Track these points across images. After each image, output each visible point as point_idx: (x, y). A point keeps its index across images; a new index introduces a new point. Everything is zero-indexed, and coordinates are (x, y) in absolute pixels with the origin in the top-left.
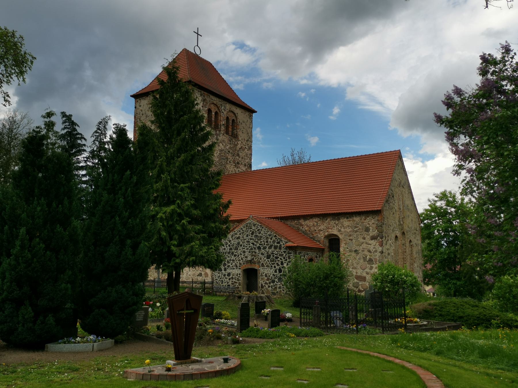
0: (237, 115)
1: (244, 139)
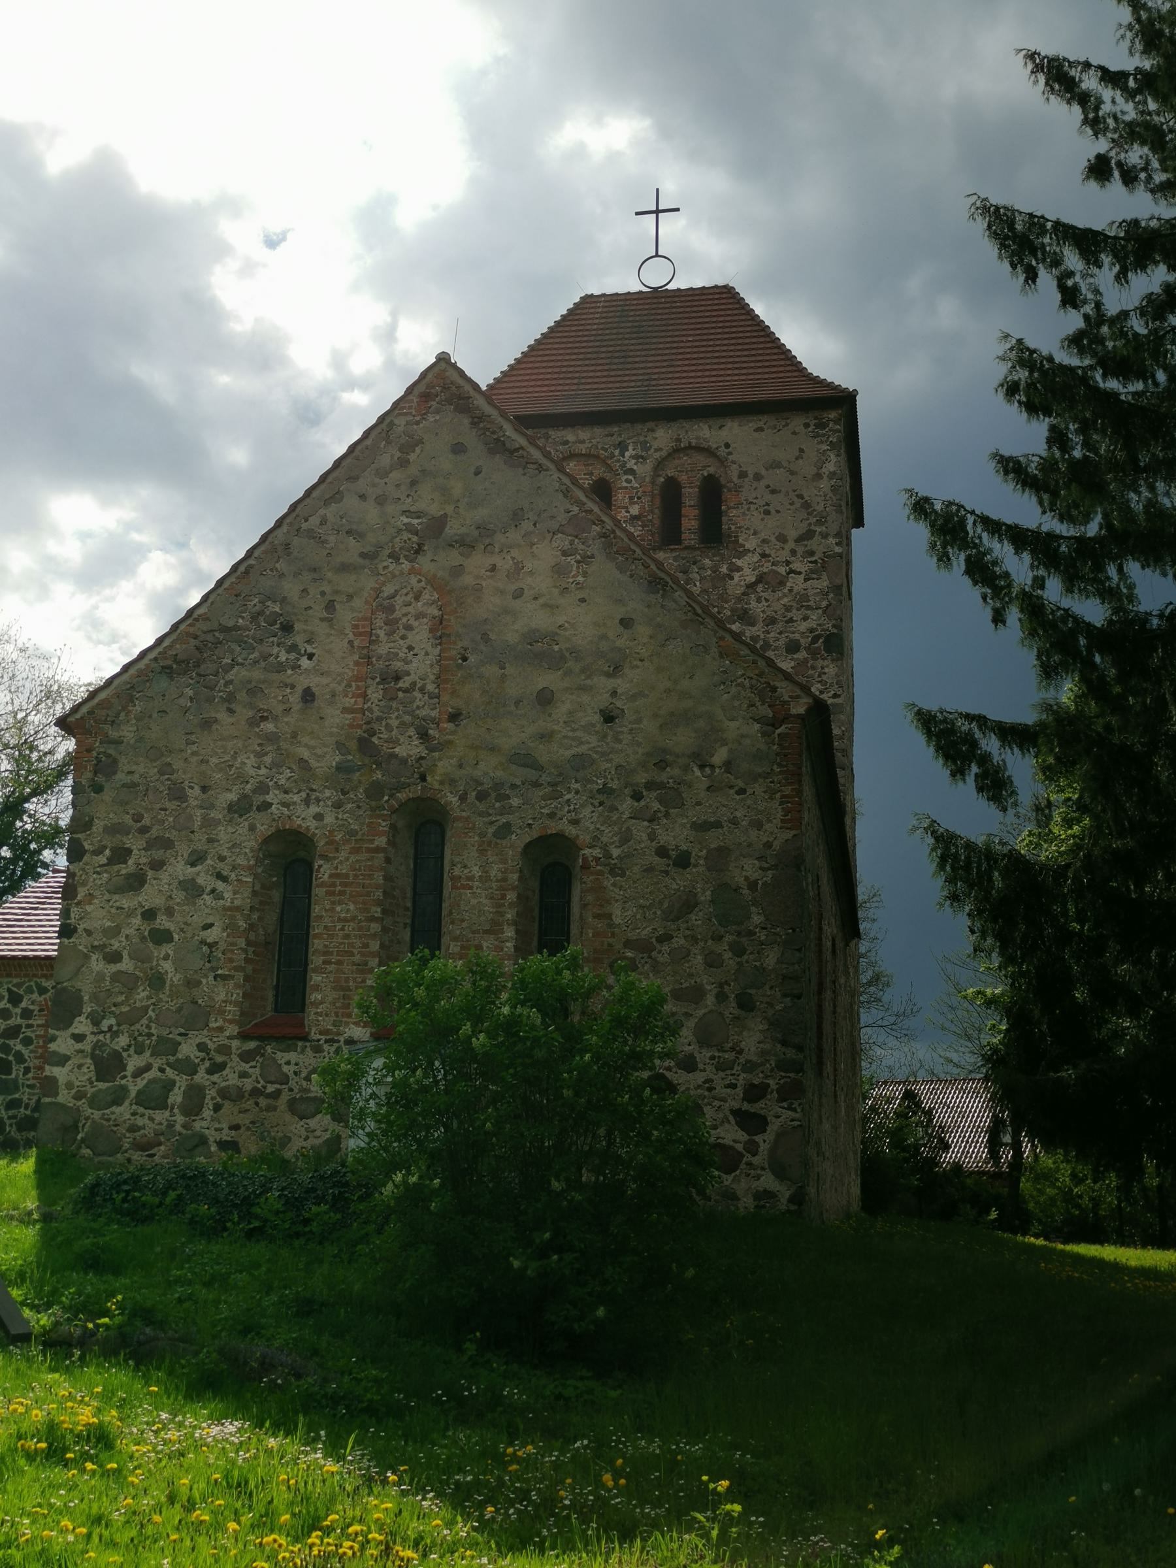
0: (722, 452)
1: (782, 539)
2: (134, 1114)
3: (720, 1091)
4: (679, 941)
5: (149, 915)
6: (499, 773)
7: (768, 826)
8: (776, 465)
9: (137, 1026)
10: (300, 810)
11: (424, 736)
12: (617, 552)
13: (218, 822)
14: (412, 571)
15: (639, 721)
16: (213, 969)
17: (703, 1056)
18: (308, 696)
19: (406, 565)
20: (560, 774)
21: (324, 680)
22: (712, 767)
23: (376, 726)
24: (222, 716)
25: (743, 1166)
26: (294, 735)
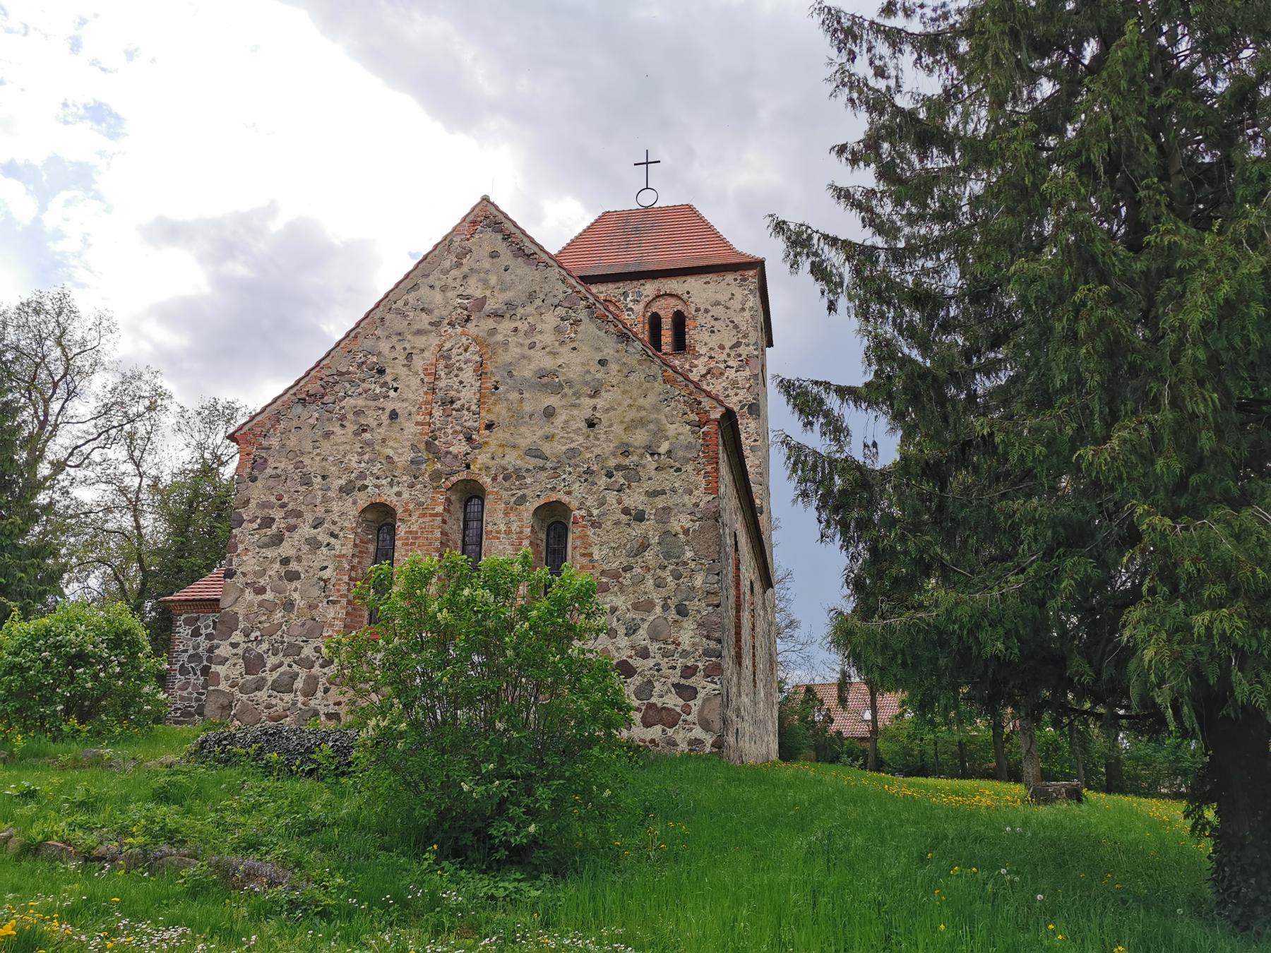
0: (685, 297)
1: (722, 347)
2: (269, 696)
3: (665, 671)
4: (637, 570)
5: (285, 561)
6: (519, 462)
7: (696, 493)
8: (717, 303)
9: (275, 636)
10: (387, 490)
11: (469, 439)
12: (597, 317)
13: (333, 499)
14: (463, 334)
15: (611, 426)
16: (327, 597)
17: (653, 647)
18: (394, 415)
19: (459, 330)
20: (559, 462)
21: (405, 405)
22: (659, 454)
23: (437, 433)
24: (338, 430)
25: (680, 722)
26: (384, 440)
